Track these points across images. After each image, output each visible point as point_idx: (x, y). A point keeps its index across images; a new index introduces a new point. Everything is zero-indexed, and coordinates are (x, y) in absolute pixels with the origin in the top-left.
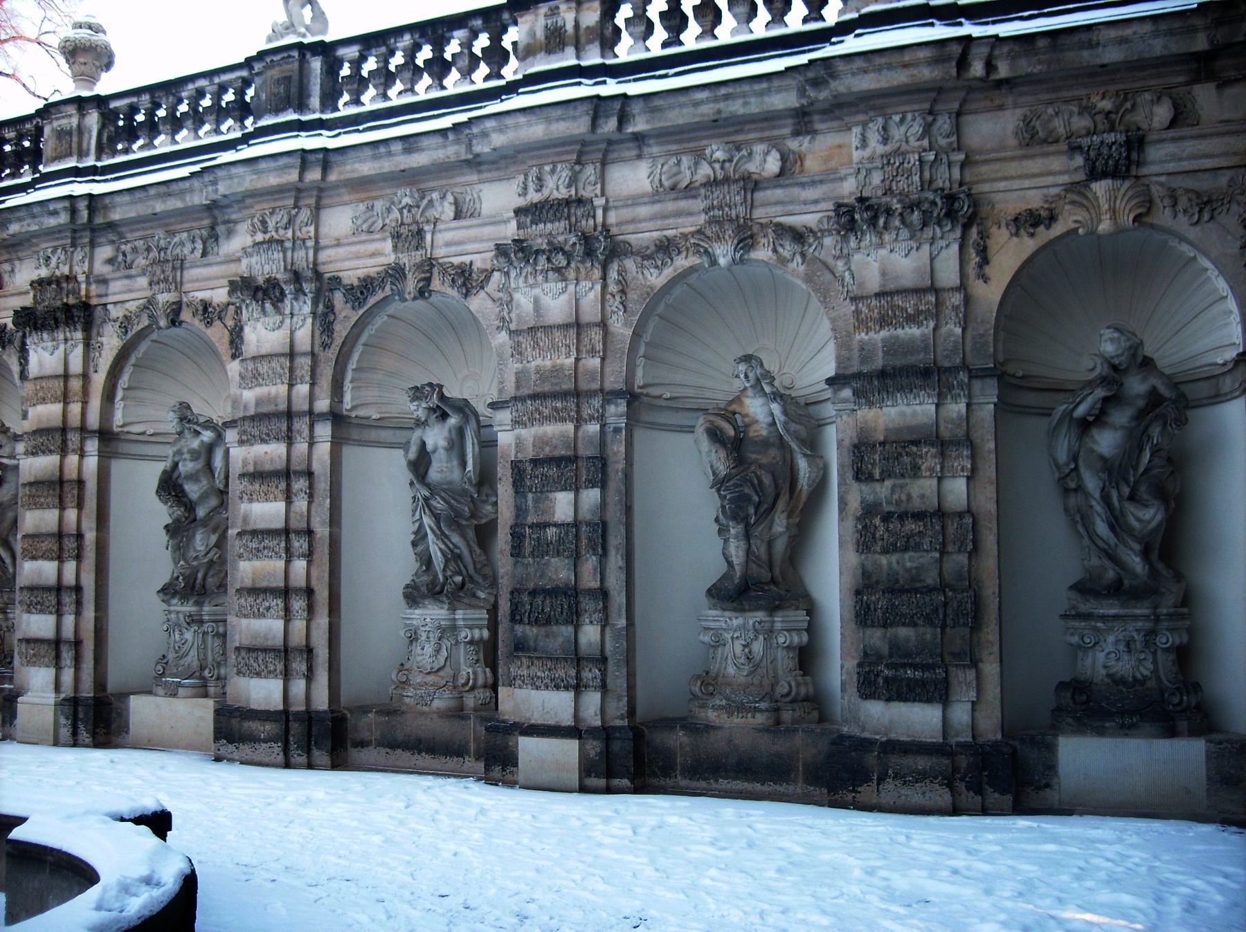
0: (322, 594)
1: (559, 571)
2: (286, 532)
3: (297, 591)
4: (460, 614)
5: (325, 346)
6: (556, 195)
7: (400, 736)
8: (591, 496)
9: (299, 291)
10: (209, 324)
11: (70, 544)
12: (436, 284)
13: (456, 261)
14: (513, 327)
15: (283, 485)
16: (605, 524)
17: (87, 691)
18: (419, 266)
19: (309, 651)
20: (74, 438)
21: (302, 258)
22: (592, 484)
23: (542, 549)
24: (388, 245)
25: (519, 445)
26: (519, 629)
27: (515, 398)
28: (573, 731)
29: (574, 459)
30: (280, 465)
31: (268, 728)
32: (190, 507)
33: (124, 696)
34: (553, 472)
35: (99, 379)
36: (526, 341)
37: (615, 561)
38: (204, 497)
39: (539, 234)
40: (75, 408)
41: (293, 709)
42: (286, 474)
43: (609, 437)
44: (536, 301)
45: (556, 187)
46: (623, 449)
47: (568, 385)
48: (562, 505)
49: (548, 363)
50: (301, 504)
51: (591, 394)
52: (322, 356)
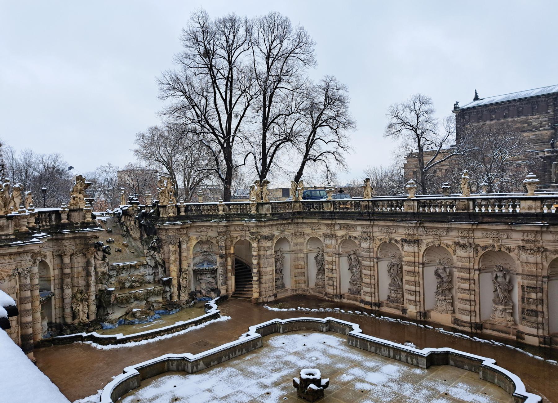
0: (477, 302)
1: (533, 307)
2: (470, 290)
3: (472, 301)
4: (507, 308)
5: (476, 256)
6: (531, 239)
7: (495, 329)
8: (540, 295)
9: (471, 247)
10: (448, 248)
11: (417, 284)
12: (502, 249)
13: (507, 246)
14: (521, 260)
15: (469, 282)
16: (543, 300)
17: (422, 310)
18: (498, 246)
19: (475, 312)
20: (417, 264)
21: (471, 240)
22: (540, 292)
23: (529, 303)
24: (491, 241)
25: (523, 282)
26: (524, 316)
27: (522, 274)
28: (537, 336)
29: (536, 288)
30: (468, 278)
31: (467, 325)
32: (442, 278)
33: (429, 311)
34: (531, 289)
35: (421, 253)
36: (524, 264)
37: (545, 306)
38: (445, 277)
39: (528, 246)
40: (417, 259)
41: (472, 321)
42: (469, 280)
43: (543, 284)
44: (527, 257)
45: (531, 237)
46: (546, 287)
47: (534, 274)
48: (533, 296)
49: (530, 269)
50: (472, 285)
51: (540, 276)
52: (475, 258)
